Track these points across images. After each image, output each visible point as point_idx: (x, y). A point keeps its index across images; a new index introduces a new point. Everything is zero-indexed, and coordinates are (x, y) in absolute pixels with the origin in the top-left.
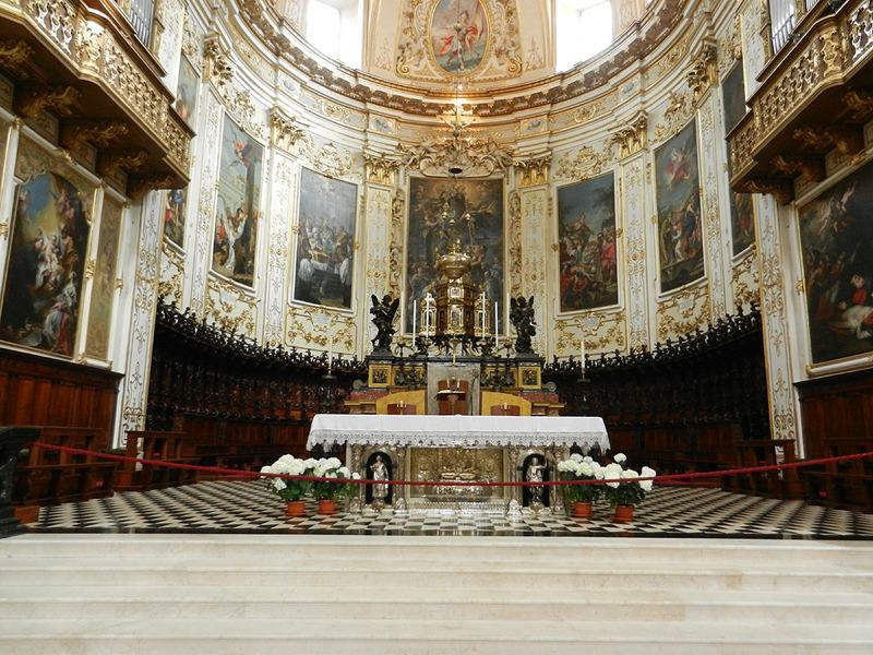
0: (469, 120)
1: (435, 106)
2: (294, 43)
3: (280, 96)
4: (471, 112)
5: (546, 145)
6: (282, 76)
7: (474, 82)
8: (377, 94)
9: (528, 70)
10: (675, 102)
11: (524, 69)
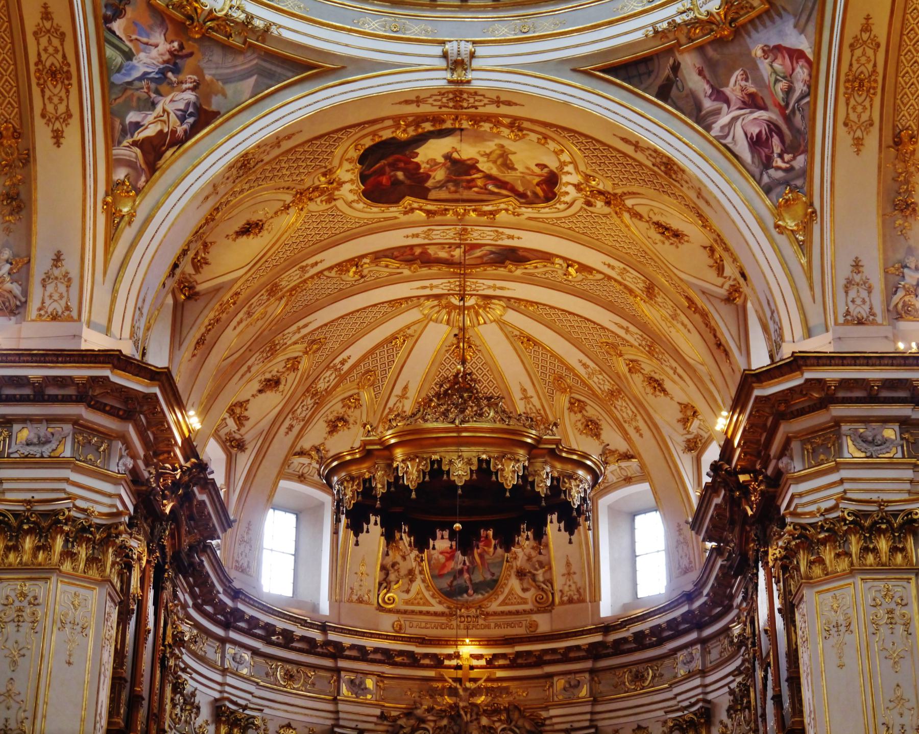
0: (483, 674)
1: (435, 656)
2: (250, 611)
3: (230, 680)
4: (483, 662)
5: (588, 717)
6: (230, 650)
7: (488, 614)
8: (353, 647)
9: (562, 603)
10: (735, 701)
11: (557, 600)
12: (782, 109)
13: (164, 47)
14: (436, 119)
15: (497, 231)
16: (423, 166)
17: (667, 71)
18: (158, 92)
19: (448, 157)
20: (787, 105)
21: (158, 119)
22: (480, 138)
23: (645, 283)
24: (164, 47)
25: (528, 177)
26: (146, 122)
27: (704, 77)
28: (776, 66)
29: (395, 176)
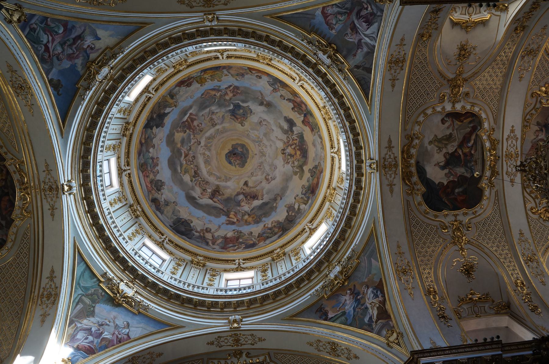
12: (349, 14)
13: (347, 297)
14: (407, 176)
15: (507, 139)
16: (451, 178)
17: (360, 70)
18: (362, 305)
19: (443, 168)
20: (345, 12)
21: (372, 308)
22: (424, 154)
23: (523, 57)
24: (347, 297)
25: (456, 127)
26: (371, 314)
27: (356, 53)
28: (334, 23)
29: (458, 193)
